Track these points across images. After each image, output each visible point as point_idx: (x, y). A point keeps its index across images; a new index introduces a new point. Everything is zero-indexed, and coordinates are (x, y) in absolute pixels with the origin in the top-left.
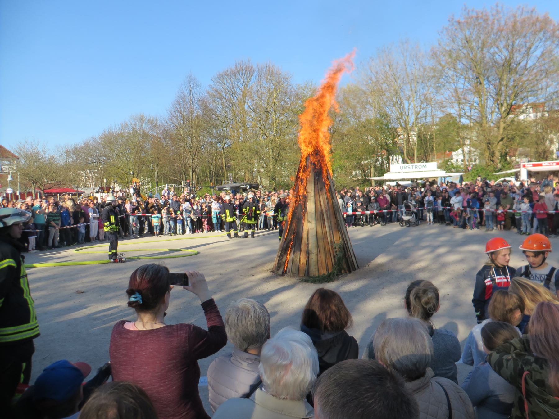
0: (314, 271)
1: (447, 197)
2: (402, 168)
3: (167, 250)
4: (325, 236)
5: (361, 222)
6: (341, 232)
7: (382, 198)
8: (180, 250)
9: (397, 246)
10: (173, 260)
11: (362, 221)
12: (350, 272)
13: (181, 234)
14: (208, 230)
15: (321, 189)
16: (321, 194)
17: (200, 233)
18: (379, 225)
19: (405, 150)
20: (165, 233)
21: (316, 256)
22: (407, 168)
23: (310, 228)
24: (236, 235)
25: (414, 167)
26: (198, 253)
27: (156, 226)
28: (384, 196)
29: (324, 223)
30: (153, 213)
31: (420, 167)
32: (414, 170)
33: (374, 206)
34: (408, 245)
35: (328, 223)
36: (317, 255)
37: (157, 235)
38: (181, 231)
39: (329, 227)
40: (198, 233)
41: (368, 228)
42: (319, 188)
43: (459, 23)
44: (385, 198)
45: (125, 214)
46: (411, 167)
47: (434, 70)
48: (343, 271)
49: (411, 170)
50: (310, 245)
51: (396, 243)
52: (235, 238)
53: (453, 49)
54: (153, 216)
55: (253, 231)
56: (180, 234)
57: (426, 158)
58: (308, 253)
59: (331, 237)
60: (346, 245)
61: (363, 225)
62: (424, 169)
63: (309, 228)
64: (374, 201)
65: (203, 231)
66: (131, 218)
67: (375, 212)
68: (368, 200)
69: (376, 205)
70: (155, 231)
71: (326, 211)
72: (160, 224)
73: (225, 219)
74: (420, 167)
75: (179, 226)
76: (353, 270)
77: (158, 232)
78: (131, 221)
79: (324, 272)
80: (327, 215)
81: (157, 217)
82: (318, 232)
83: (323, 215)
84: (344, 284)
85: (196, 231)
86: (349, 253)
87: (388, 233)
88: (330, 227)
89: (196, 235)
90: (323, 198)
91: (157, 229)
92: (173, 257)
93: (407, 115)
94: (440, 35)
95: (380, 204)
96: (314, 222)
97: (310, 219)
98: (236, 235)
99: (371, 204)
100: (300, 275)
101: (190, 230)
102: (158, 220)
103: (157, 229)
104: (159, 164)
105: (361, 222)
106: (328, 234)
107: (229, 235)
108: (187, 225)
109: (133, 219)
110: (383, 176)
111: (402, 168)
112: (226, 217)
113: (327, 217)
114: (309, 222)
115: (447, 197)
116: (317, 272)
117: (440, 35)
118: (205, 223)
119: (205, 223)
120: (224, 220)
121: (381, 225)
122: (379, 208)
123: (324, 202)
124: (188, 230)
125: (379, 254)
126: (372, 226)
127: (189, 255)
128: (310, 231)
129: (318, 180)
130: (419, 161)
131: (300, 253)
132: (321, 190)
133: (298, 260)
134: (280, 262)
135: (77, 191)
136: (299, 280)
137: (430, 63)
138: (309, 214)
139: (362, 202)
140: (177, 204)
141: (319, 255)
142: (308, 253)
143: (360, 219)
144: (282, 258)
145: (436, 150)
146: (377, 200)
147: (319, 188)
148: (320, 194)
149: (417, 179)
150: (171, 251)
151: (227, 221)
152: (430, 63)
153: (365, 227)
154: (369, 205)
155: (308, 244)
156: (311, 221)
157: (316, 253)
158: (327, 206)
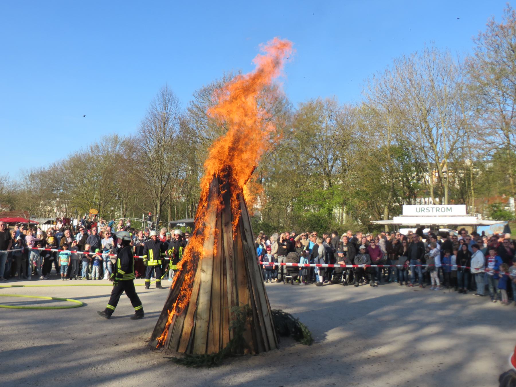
0: (200, 348)
2: (418, 210)
3: (51, 298)
4: (223, 295)
5: (343, 279)
6: (250, 289)
7: (373, 247)
8: (65, 300)
9: (371, 317)
10: (46, 312)
11: (345, 278)
12: (257, 353)
13: (97, 278)
15: (227, 224)
16: (226, 232)
18: (368, 286)
21: (207, 324)
22: (426, 210)
23: (203, 280)
24: (158, 284)
25: (435, 210)
26: (84, 305)
27: (64, 266)
28: (375, 245)
29: (225, 275)
31: (443, 210)
32: (435, 213)
33: (363, 259)
34: (386, 318)
35: (231, 274)
36: (209, 322)
37: (64, 278)
38: (97, 274)
39: (232, 281)
41: (352, 289)
42: (224, 221)
43: (502, 28)
45: (23, 248)
46: (431, 210)
47: (470, 87)
48: (246, 351)
49: (430, 214)
50: (200, 306)
51: (372, 313)
52: (157, 289)
53: (497, 62)
54: (61, 252)
55: (147, 280)
56: (95, 279)
57: (464, 201)
58: (195, 316)
59: (232, 297)
60: (256, 310)
61: (345, 284)
62: (449, 213)
63: (202, 281)
64: (364, 251)
66: (32, 254)
67: (363, 266)
68: (354, 250)
69: (365, 258)
70: (62, 273)
71: (231, 257)
72: (68, 264)
73: (147, 262)
74: (443, 210)
75: (96, 268)
76: (265, 350)
77: (65, 274)
78: (31, 257)
79: (214, 349)
80: (231, 262)
81: (66, 254)
82: (214, 288)
83: (225, 262)
84: (234, 372)
86: (261, 324)
87: (378, 296)
88: (235, 281)
90: (229, 237)
92: (55, 309)
94: (476, 43)
95: (370, 256)
96: (209, 272)
97: (204, 267)
98: (158, 284)
99: (359, 255)
102: (68, 258)
105: (343, 279)
106: (229, 291)
107: (148, 284)
108: (107, 268)
109: (34, 256)
110: (392, 219)
111: (418, 210)
112: (148, 259)
113: (231, 266)
114: (203, 271)
116: (204, 349)
117: (476, 43)
120: (145, 263)
121: (371, 286)
122: (369, 262)
123: (228, 243)
125: (331, 328)
126: (358, 286)
127: (64, 307)
128: (203, 284)
129: (223, 210)
130: (449, 203)
131: (185, 317)
132: (225, 226)
133: (181, 327)
134: (158, 327)
135: (29, 221)
136: (167, 359)
137: (465, 79)
140: (96, 240)
141: (211, 323)
142: (195, 316)
143: (341, 273)
144: (161, 323)
145: (474, 189)
146: (368, 250)
147: (224, 221)
148: (224, 230)
149: (438, 227)
150: (55, 300)
151: (149, 264)
152: (465, 79)
153: (349, 286)
154: (356, 257)
155: (197, 304)
156: (205, 270)
157: (207, 319)
158: (232, 250)
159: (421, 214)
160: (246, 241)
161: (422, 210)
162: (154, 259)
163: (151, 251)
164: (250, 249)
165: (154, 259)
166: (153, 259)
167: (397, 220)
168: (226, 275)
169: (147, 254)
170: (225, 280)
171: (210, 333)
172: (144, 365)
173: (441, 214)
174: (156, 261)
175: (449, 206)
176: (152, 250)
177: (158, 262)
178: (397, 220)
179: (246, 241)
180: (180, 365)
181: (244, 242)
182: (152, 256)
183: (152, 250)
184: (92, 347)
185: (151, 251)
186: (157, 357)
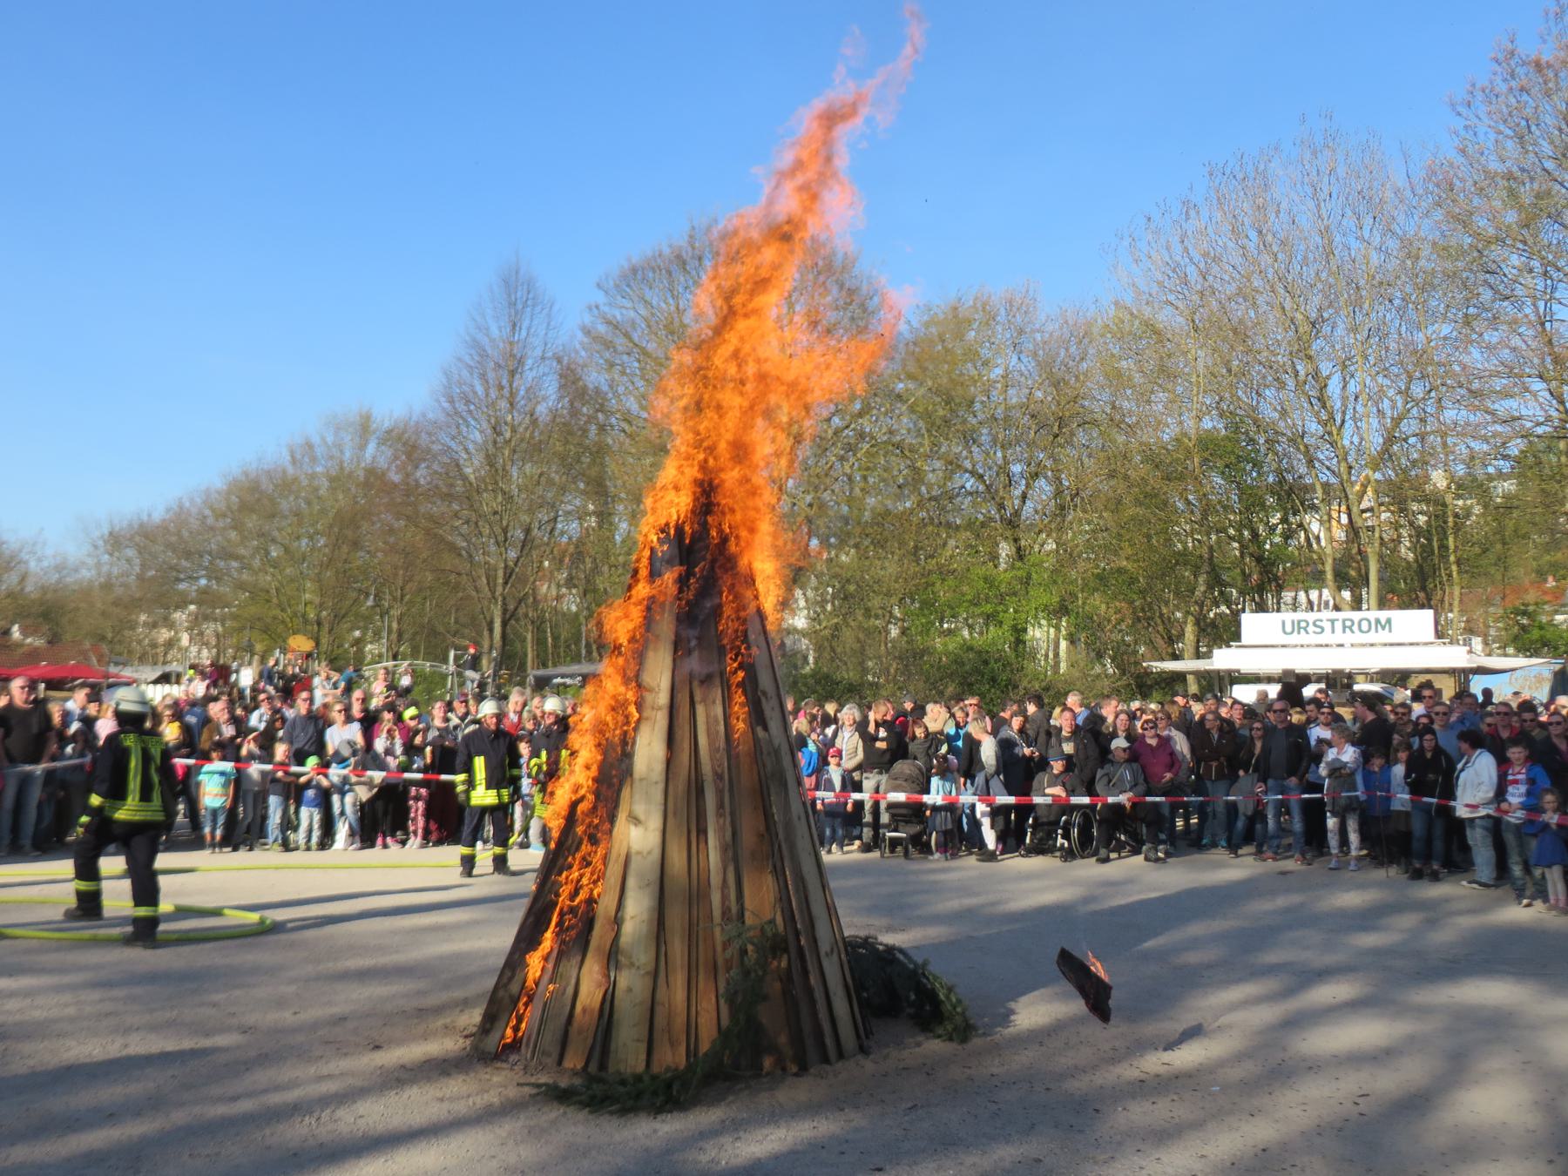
0: (629, 1055)
1: (1429, 755)
2: (1288, 629)
4: (697, 894)
5: (1060, 841)
6: (778, 873)
7: (1153, 742)
8: (216, 913)
11: (1066, 836)
12: (803, 1069)
14: (434, 837)
16: (704, 701)
17: (394, 848)
18: (1139, 859)
19: (1330, 561)
20: (213, 837)
21: (649, 981)
22: (1311, 628)
23: (635, 847)
24: (500, 863)
25: (1338, 625)
27: (215, 813)
28: (1158, 736)
29: (702, 832)
30: (206, 758)
31: (1365, 625)
32: (1339, 637)
33: (1121, 779)
34: (1193, 958)
37: (213, 845)
39: (724, 849)
40: (385, 846)
41: (1088, 869)
44: (1165, 742)
46: (1327, 626)
47: (1443, 251)
48: (767, 1062)
52: (497, 877)
53: (1523, 170)
54: (207, 768)
55: (465, 850)
56: (308, 849)
57: (1429, 600)
58: (613, 957)
59: (724, 898)
61: (1069, 855)
62: (1383, 636)
63: (633, 851)
64: (1123, 756)
65: (403, 843)
67: (1123, 799)
68: (1093, 751)
70: (207, 830)
71: (718, 776)
72: (228, 805)
73: (467, 792)
74: (1365, 625)
75: (309, 816)
76: (826, 1060)
77: (218, 833)
79: (672, 1057)
80: (719, 793)
81: (222, 774)
83: (700, 792)
84: (735, 1127)
85: (379, 841)
86: (814, 980)
88: (732, 852)
89: (375, 854)
91: (214, 821)
93: (1338, 422)
95: (1143, 768)
96: (655, 822)
97: (639, 809)
98: (500, 863)
99: (1108, 768)
100: (569, 1063)
101: (352, 834)
102: (225, 785)
103: (214, 821)
104: (407, 588)
105: (1060, 841)
106: (715, 880)
107: (468, 863)
108: (342, 813)
110: (1208, 655)
111: (1288, 629)
112: (471, 784)
113: (720, 805)
114: (636, 820)
115: (1429, 755)
116: (643, 1057)
118: (418, 809)
119: (418, 809)
120: (462, 797)
121: (1147, 859)
122: (1141, 788)
124: (342, 831)
126: (1106, 860)
130: (1383, 604)
134: (501, 993)
135: (107, 676)
136: (527, 1090)
138: (637, 784)
139: (1069, 758)
140: (311, 729)
142: (613, 957)
144: (511, 979)
145: (1458, 562)
148: (697, 698)
149: (1350, 677)
152: (1426, 227)
153: (1079, 862)
154: (1100, 773)
155: (617, 921)
156: (642, 817)
157: (651, 967)
159: (1295, 639)
160: (766, 728)
161: (1299, 627)
162: (488, 787)
163: (479, 763)
164: (777, 752)
165: (488, 787)
166: (484, 786)
167: (1223, 659)
168: (705, 833)
169: (469, 769)
170: (702, 846)
171: (659, 1010)
172: (461, 1108)
174: (493, 792)
175: (1383, 615)
176: (482, 758)
177: (499, 795)
178: (1223, 659)
179: (766, 728)
180: (467, 1074)
181: (759, 730)
182: (484, 776)
183: (482, 758)
184: (302, 1054)
185: (479, 763)
186: (498, 1084)
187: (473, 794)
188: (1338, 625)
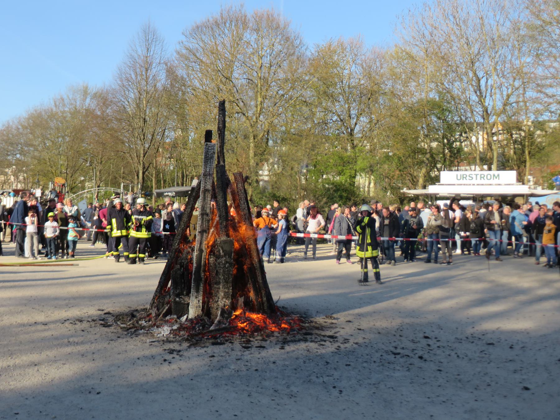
2: (459, 178)
22: (468, 178)
25: (479, 177)
32: (479, 181)
46: (474, 177)
49: (474, 181)
62: (496, 181)
110: (424, 187)
111: (459, 178)
112: (112, 229)
159: (461, 182)
161: (463, 177)
162: (118, 230)
163: (114, 221)
165: (118, 230)
166: (116, 229)
167: (432, 189)
169: (110, 223)
173: (486, 182)
174: (119, 231)
175: (496, 173)
176: (115, 219)
177: (121, 233)
178: (432, 189)
183: (115, 219)
185: (114, 221)
187: (113, 232)
188: (479, 177)
